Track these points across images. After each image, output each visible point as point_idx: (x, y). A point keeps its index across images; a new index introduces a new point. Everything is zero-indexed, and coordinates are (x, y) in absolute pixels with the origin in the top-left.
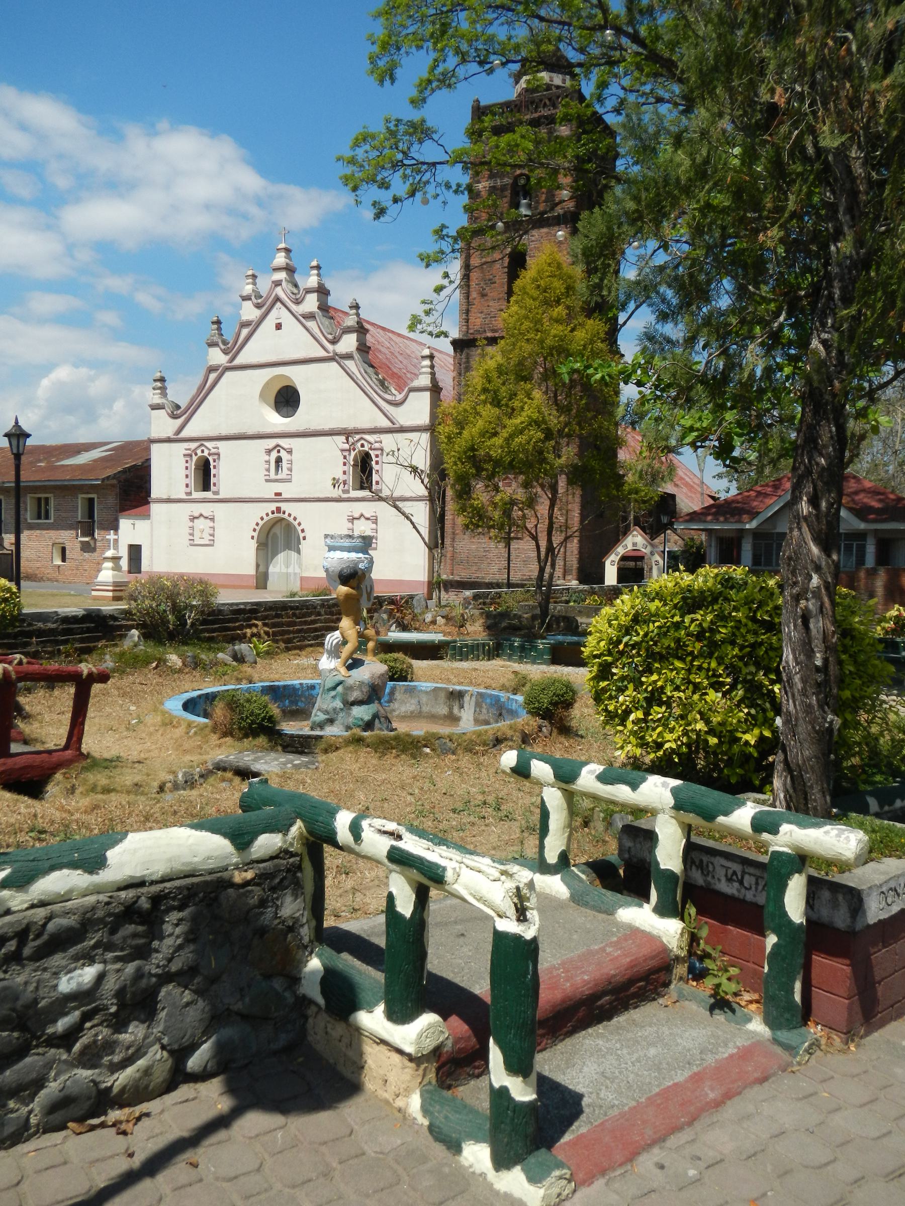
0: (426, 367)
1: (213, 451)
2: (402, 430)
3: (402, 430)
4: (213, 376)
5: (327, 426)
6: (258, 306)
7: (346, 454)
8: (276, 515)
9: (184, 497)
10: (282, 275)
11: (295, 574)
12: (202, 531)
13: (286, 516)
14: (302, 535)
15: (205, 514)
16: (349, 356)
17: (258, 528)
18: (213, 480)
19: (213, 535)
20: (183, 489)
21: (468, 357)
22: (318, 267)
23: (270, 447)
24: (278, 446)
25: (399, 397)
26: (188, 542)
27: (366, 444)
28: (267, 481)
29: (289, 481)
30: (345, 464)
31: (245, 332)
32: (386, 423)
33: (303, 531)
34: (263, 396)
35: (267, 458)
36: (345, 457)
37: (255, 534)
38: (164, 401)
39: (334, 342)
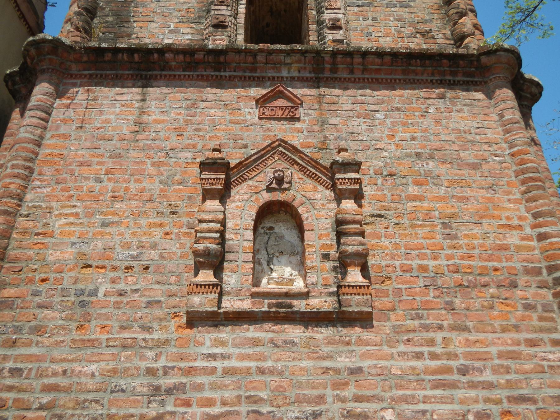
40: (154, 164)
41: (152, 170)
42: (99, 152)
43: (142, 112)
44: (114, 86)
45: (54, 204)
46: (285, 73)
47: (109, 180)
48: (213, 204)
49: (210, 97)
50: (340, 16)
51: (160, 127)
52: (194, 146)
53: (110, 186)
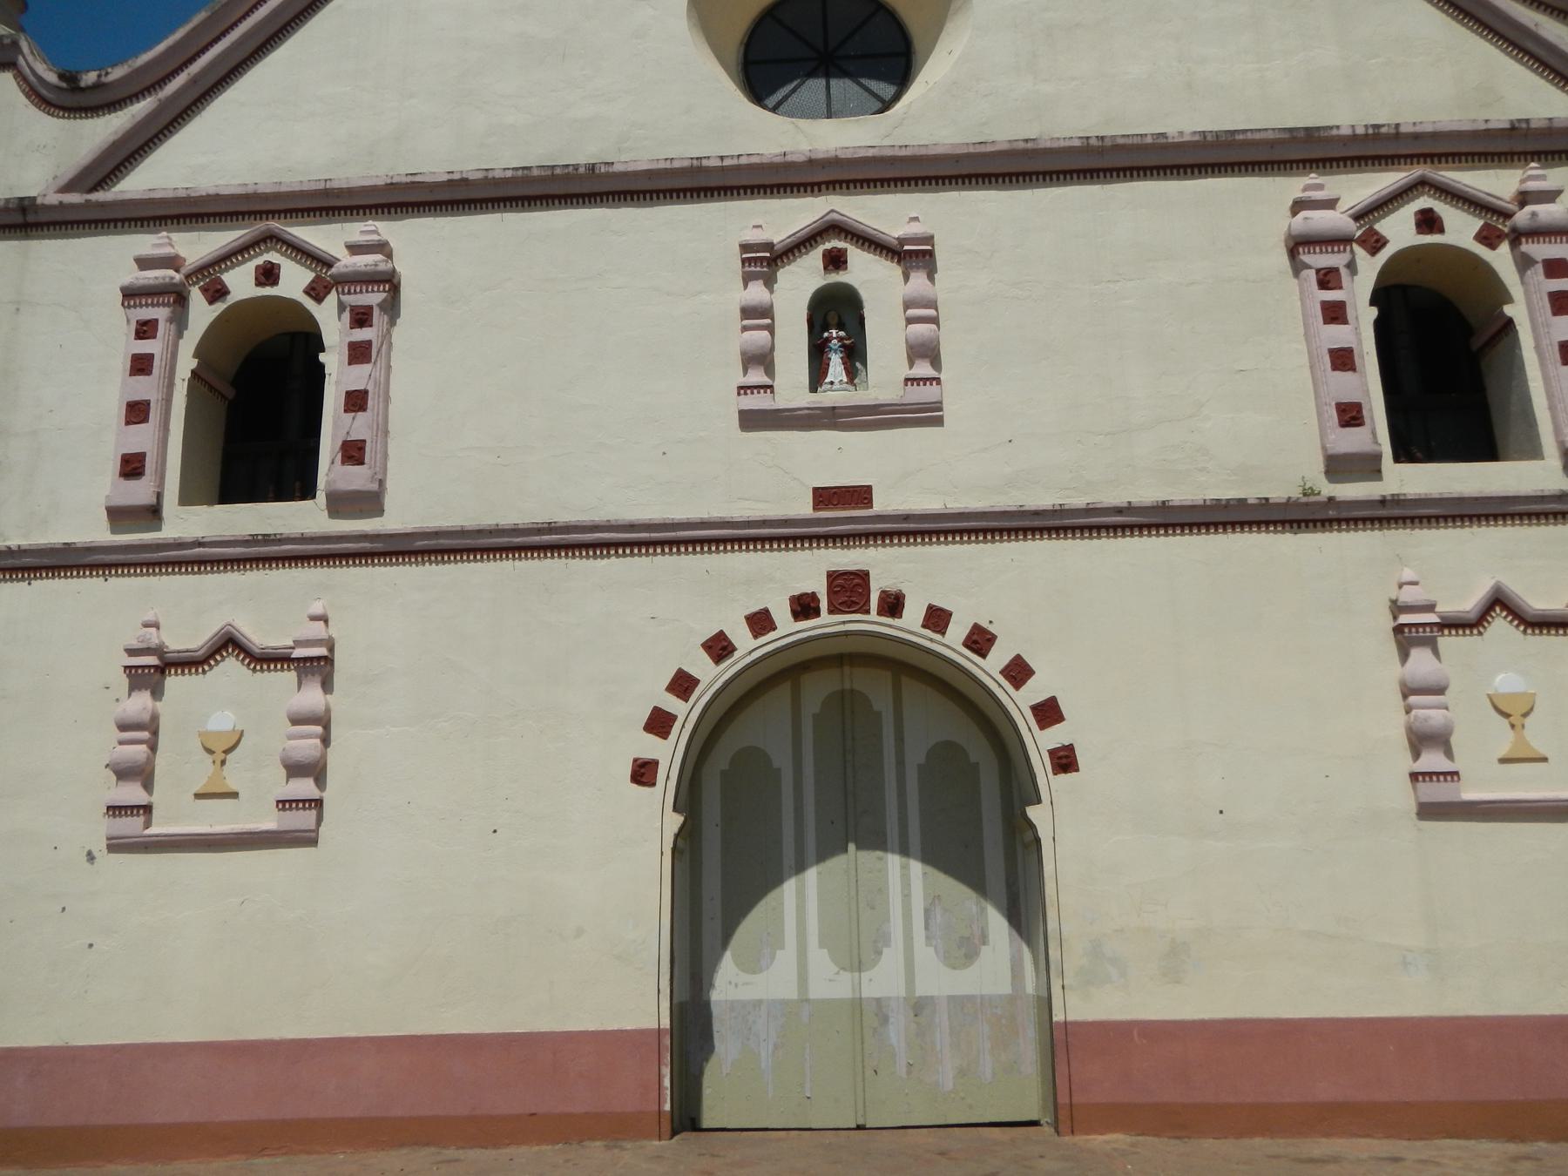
1: (347, 262)
8: (827, 622)
9: (98, 533)
11: (919, 1007)
12: (224, 749)
14: (1040, 743)
15: (261, 638)
17: (686, 712)
18: (334, 425)
19: (316, 770)
20: (107, 486)
24: (833, 228)
26: (101, 829)
28: (751, 421)
29: (928, 415)
30: (1335, 313)
33: (1048, 713)
35: (757, 293)
36: (1328, 279)
37: (668, 753)
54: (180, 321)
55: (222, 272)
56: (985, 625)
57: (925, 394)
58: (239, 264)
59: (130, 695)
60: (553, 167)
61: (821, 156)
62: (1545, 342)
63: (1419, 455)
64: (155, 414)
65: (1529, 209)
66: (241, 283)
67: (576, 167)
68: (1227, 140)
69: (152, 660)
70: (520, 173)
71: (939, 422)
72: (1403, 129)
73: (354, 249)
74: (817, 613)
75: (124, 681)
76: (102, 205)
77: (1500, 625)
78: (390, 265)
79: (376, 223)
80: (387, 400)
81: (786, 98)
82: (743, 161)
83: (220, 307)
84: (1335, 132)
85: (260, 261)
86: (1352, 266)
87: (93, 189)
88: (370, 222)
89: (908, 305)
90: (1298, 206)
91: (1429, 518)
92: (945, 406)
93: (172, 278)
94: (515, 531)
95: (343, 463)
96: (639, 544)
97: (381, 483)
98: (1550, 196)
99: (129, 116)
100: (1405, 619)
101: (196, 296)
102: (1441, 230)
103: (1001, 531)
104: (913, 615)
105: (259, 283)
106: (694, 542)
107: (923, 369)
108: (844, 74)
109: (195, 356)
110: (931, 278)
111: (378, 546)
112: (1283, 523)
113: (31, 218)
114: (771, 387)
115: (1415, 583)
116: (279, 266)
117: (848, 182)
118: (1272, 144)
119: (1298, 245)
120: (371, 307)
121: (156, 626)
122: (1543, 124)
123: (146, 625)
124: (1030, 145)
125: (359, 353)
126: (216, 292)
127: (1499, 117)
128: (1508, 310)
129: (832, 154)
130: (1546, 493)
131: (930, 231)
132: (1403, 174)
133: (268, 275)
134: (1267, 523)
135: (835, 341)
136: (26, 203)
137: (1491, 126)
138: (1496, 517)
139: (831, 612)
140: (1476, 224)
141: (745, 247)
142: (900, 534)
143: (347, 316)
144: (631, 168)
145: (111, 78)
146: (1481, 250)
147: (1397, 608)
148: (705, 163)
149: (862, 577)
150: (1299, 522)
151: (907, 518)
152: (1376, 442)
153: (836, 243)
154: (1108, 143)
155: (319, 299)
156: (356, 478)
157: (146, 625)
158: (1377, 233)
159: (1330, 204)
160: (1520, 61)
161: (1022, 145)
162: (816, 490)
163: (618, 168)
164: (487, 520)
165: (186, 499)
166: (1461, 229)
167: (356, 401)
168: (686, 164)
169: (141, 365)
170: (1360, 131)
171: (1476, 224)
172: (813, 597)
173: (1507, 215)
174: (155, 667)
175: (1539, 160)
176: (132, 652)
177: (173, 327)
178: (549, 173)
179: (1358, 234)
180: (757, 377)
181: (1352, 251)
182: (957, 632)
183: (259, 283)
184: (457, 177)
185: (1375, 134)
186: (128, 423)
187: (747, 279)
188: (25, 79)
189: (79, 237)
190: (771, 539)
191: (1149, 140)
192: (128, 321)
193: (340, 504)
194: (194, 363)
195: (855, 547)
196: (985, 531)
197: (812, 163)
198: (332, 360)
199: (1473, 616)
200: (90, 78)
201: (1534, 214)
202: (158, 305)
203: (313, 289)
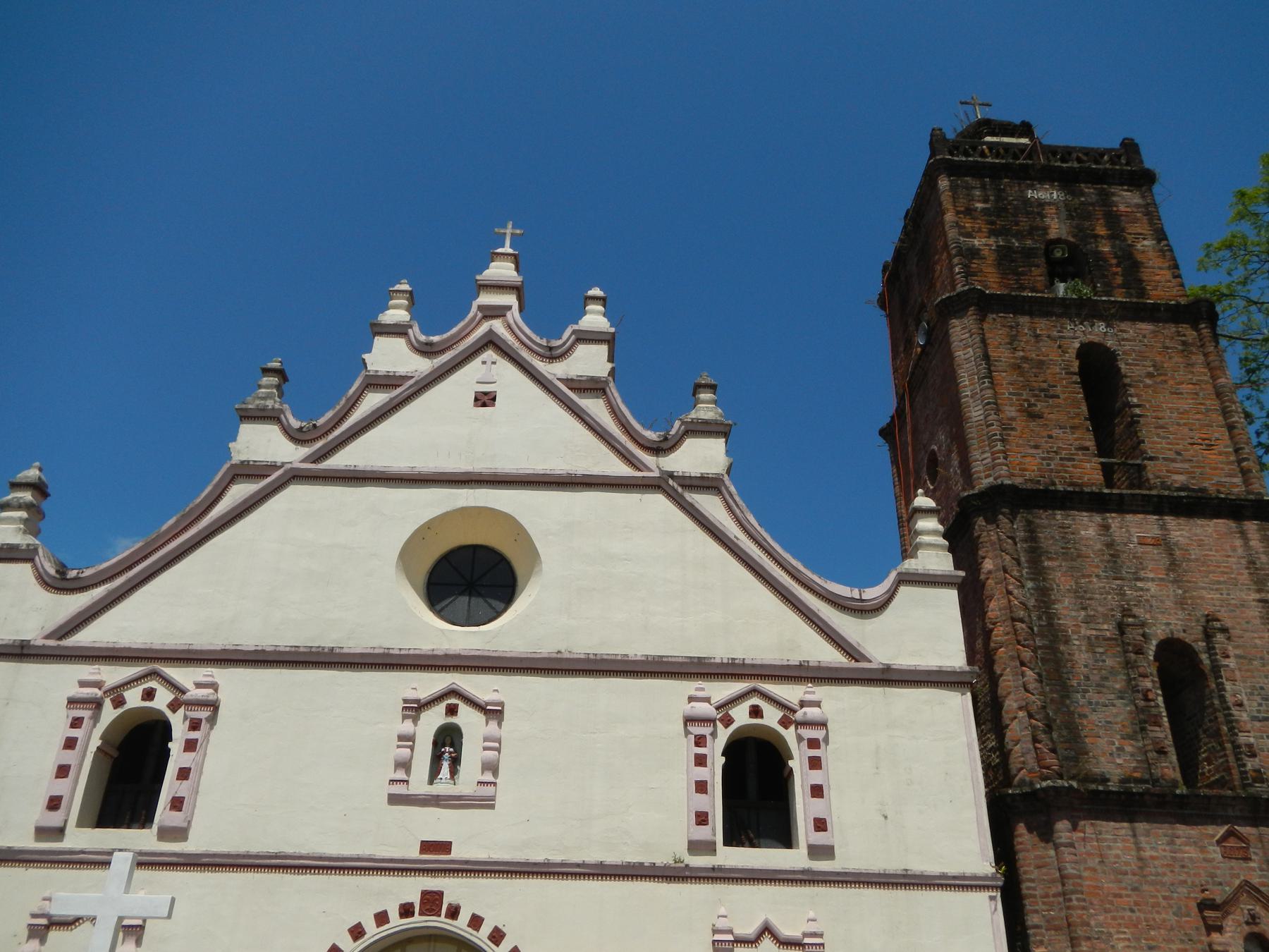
0: (934, 532)
1: (194, 693)
2: (889, 677)
3: (889, 677)
4: (239, 492)
5: (638, 649)
6: (426, 350)
7: (705, 730)
8: (418, 920)
9: (25, 841)
10: (510, 300)
13: (460, 925)
16: (707, 484)
18: (170, 786)
20: (37, 814)
21: (1031, 530)
22: (602, 300)
23: (424, 694)
25: (873, 593)
27: (766, 707)
28: (394, 799)
29: (487, 803)
30: (701, 761)
31: (374, 400)
32: (830, 656)
34: (407, 555)
35: (408, 727)
36: (700, 741)
38: (30, 540)
39: (658, 449)
40: (1165, 898)
41: (1164, 903)
42: (1123, 885)
43: (1139, 849)
44: (1108, 820)
45: (1112, 930)
46: (1230, 812)
47: (1139, 910)
48: (1215, 936)
49: (1180, 832)
50: (1252, 740)
51: (1156, 862)
52: (1185, 882)
53: (1142, 916)
54: (96, 719)
55: (124, 691)
56: (501, 927)
57: (488, 791)
58: (135, 687)
59: (27, 940)
60: (312, 647)
61: (451, 653)
62: (805, 783)
63: (752, 835)
64: (72, 773)
65: (805, 709)
66: (133, 698)
67: (323, 648)
68: (659, 660)
69: (44, 921)
70: (293, 649)
71: (492, 807)
72: (746, 662)
73: (199, 685)
74: (412, 914)
75: (26, 933)
76: (67, 648)
77: (767, 943)
78: (215, 697)
79: (213, 669)
80: (201, 773)
81: (447, 606)
82: (411, 652)
83: (120, 711)
84: (712, 661)
85: (146, 686)
86: (714, 734)
87: (60, 639)
88: (209, 669)
89: (486, 740)
90: (691, 699)
91: (737, 879)
92: (497, 799)
93: (96, 695)
94: (257, 856)
95: (170, 809)
96: (323, 868)
97: (189, 822)
98: (817, 704)
99: (90, 597)
100: (718, 937)
101: (108, 703)
102: (762, 717)
103: (516, 873)
104: (464, 917)
105: (143, 699)
106: (353, 868)
107: (488, 777)
108: (480, 595)
109: (101, 738)
110: (500, 725)
111: (181, 860)
112: (662, 877)
113: (25, 651)
114: (407, 782)
115: (726, 917)
116: (156, 690)
117: (464, 667)
118: (682, 664)
119: (689, 720)
120: (201, 720)
121: (49, 899)
122: (816, 664)
123: (45, 899)
124: (559, 656)
125: (190, 746)
126: (119, 702)
127: (795, 659)
128: (791, 763)
129: (457, 652)
130: (796, 869)
131: (502, 699)
132: (747, 684)
133: (149, 695)
134: (654, 877)
135: (447, 754)
136: (25, 643)
137: (790, 663)
138: (771, 880)
139: (420, 914)
140: (779, 714)
141: (405, 701)
142: (462, 871)
143: (187, 723)
144: (352, 651)
145: (83, 575)
146: (780, 729)
147: (715, 931)
148: (391, 652)
149: (440, 895)
150: (671, 877)
151: (467, 862)
152: (715, 835)
153: (453, 701)
154: (598, 657)
155: (174, 711)
156: (175, 819)
157: (45, 899)
158: (729, 716)
159: (707, 700)
160: (811, 627)
161: (555, 655)
162: (422, 842)
163: (346, 651)
164: (242, 849)
165: (81, 824)
166: (771, 717)
167: (184, 774)
168: (381, 651)
169: (70, 744)
170: (725, 661)
171: (779, 714)
172: (411, 905)
173: (794, 711)
174: (45, 925)
175: (811, 682)
176: (34, 916)
177: (92, 721)
178: (309, 650)
179: (718, 717)
180: (401, 775)
181: (715, 726)
182: (486, 930)
183: (143, 699)
184: (260, 648)
185: (733, 663)
186: (57, 777)
187: (405, 717)
188: (37, 569)
189: (50, 663)
190: (394, 870)
191: (619, 658)
192: (68, 717)
193: (167, 834)
194: (99, 743)
195: (438, 877)
196: (508, 872)
197: (446, 656)
198: (175, 747)
199: (753, 937)
200: (72, 574)
201: (805, 713)
202: (86, 709)
203: (172, 705)
